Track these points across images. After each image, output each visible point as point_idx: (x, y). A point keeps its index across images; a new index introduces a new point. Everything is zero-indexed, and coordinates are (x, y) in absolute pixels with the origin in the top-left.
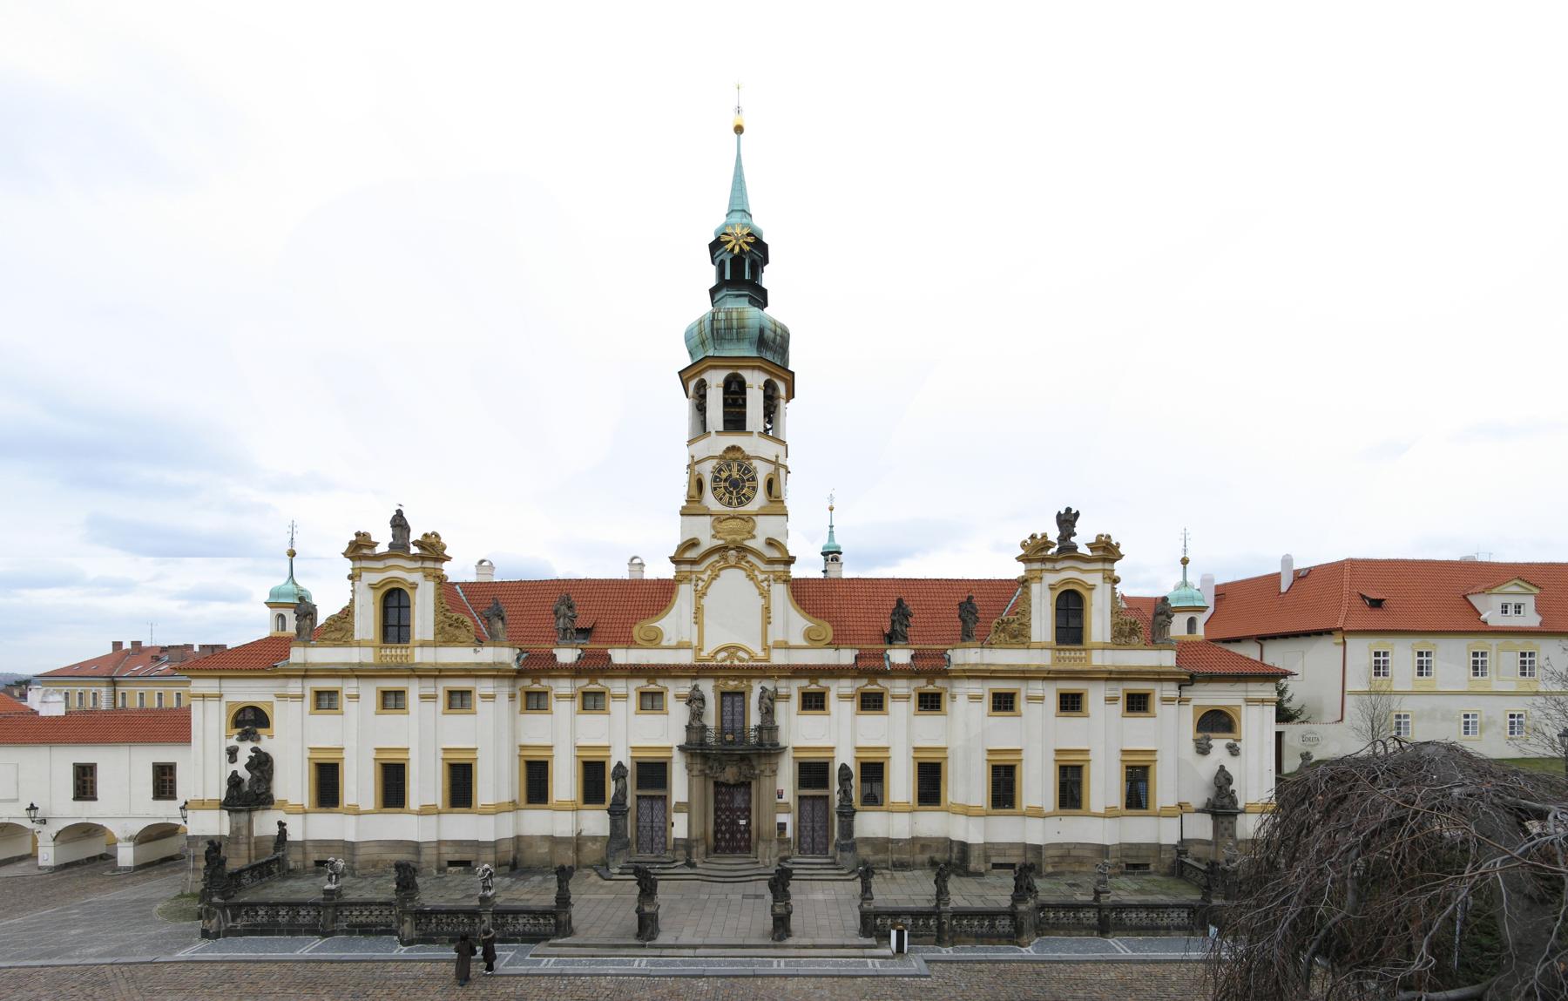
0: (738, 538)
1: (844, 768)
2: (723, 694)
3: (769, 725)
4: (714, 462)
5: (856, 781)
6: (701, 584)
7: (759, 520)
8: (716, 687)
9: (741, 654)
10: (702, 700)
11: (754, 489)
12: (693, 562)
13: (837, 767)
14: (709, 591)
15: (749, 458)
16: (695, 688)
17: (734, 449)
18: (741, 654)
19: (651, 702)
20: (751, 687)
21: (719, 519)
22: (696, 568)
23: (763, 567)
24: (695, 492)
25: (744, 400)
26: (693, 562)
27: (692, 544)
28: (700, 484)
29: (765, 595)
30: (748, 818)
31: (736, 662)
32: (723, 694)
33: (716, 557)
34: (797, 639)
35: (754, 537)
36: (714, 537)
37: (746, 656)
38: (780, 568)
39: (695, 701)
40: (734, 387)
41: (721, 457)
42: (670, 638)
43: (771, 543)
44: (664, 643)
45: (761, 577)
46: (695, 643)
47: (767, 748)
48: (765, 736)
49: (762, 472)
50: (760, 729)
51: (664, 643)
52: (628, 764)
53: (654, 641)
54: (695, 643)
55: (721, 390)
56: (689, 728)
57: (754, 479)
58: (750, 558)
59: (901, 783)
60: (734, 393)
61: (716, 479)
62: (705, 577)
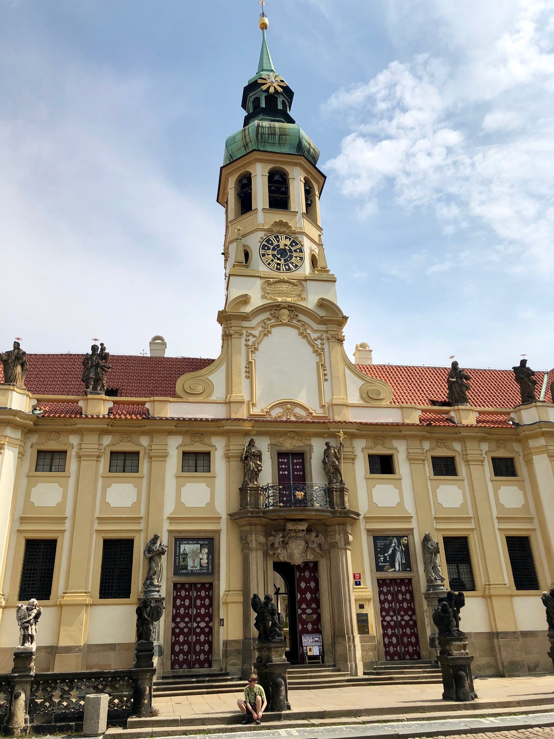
0: (289, 299)
1: (426, 539)
2: (281, 455)
3: (335, 490)
4: (261, 234)
5: (441, 559)
6: (252, 339)
7: (310, 285)
8: (271, 445)
9: (298, 410)
10: (259, 456)
11: (301, 259)
12: (246, 317)
13: (417, 540)
14: (261, 347)
15: (294, 233)
16: (251, 444)
17: (281, 223)
18: (298, 410)
19: (196, 462)
20: (311, 446)
21: (268, 282)
22: (245, 324)
23: (315, 326)
24: (243, 259)
25: (287, 188)
26: (246, 317)
27: (244, 300)
28: (247, 255)
29: (318, 352)
30: (317, 611)
31: (293, 419)
32: (281, 455)
33: (266, 315)
34: (354, 398)
35: (304, 299)
36: (263, 297)
37: (303, 413)
38: (334, 327)
39: (249, 460)
40: (277, 178)
41: (269, 230)
42: (219, 393)
43: (323, 304)
44: (213, 398)
45: (314, 336)
46: (247, 398)
47: (339, 516)
48: (336, 499)
49: (308, 246)
50: (328, 492)
51: (213, 398)
52: (164, 540)
53: (201, 395)
54: (247, 398)
55: (266, 179)
56: (243, 490)
57: (301, 251)
58: (302, 317)
59: (492, 563)
60: (277, 182)
61: (264, 247)
62: (256, 333)
